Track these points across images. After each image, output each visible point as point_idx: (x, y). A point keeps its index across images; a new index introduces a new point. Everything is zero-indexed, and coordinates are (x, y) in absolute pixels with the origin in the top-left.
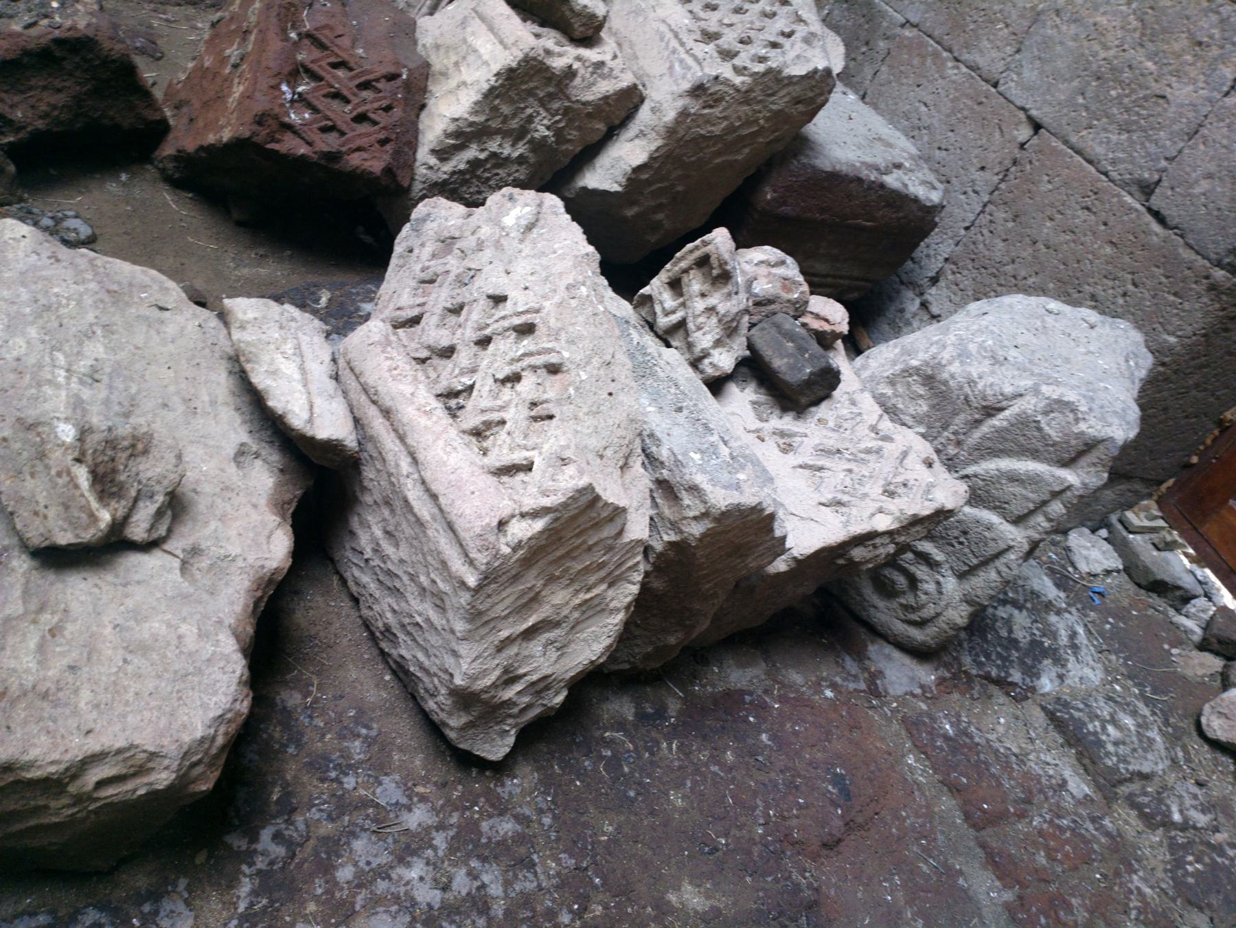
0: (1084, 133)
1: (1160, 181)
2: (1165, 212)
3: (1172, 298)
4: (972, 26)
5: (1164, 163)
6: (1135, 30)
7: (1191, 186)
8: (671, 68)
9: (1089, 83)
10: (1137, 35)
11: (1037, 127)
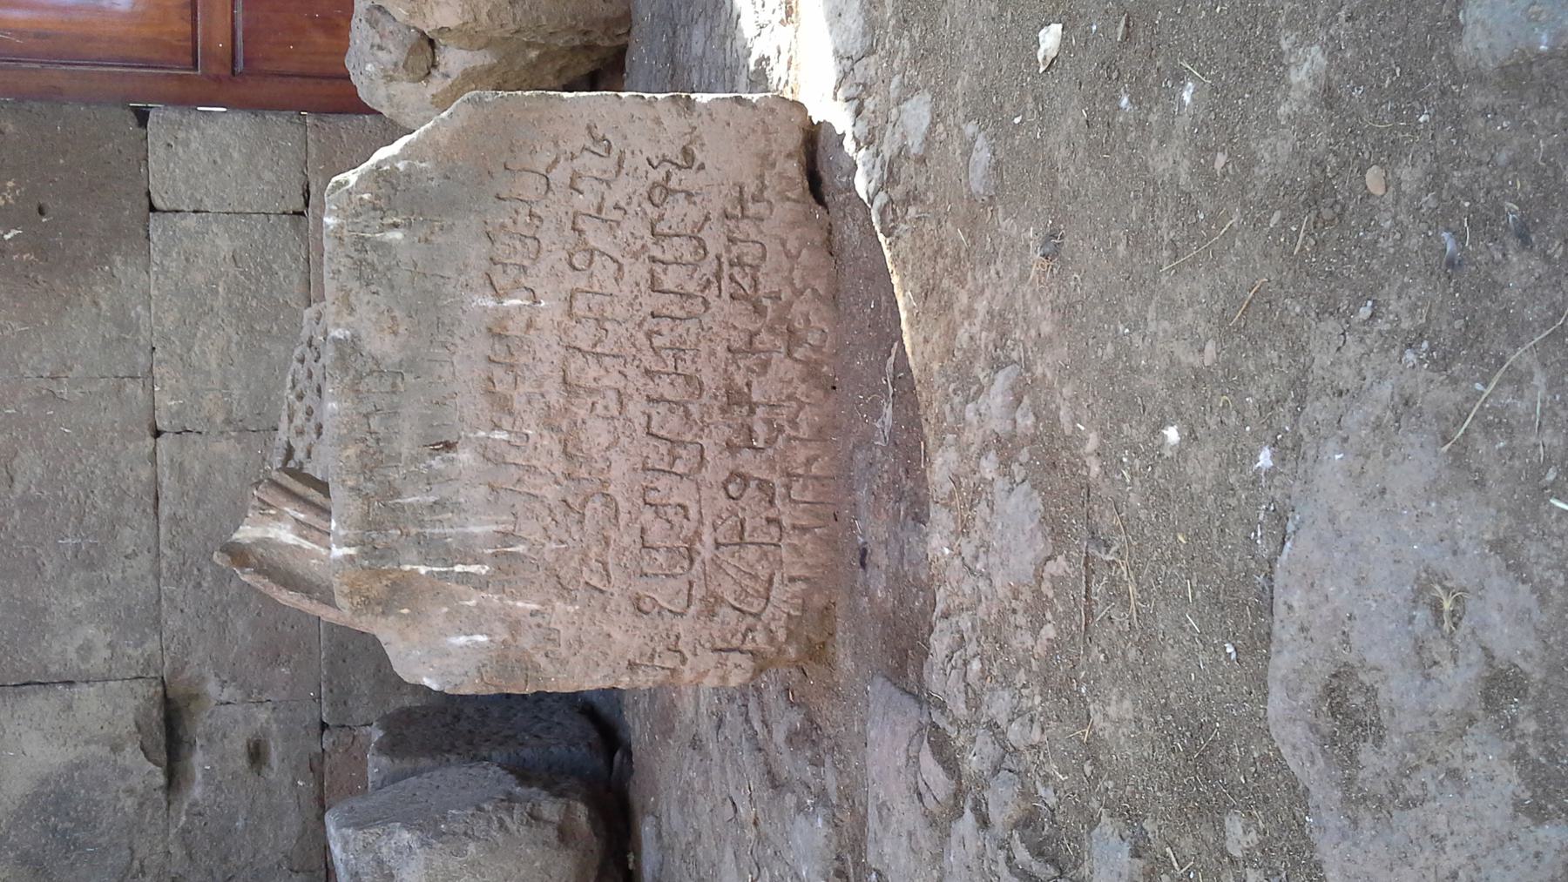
0: (293, 305)
3: (344, 136)
6: (206, 324)
7: (273, 184)
9: (260, 331)
10: (207, 319)
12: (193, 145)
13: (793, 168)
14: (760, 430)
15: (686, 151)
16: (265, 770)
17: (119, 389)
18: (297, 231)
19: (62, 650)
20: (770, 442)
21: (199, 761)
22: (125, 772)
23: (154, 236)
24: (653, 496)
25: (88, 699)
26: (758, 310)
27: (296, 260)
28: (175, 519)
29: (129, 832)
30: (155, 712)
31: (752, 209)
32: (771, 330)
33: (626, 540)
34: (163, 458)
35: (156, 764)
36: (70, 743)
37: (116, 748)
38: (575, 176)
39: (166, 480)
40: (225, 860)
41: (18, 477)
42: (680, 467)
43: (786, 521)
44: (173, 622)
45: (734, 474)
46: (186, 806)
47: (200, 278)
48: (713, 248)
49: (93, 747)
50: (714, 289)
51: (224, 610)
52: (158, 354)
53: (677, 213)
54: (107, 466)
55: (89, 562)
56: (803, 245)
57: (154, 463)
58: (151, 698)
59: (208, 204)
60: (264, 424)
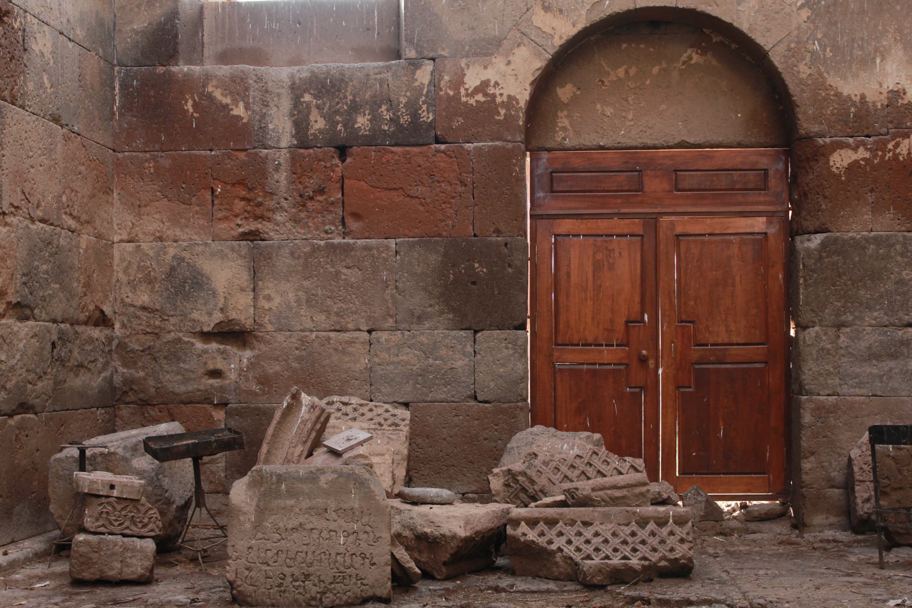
0: (430, 395)
1: (475, 392)
2: (487, 399)
4: (337, 388)
5: (472, 386)
8: (389, 438)
10: (424, 355)
12: (505, 350)
13: (370, 593)
14: (297, 584)
15: (374, 564)
16: (207, 377)
17: (391, 316)
18: (466, 398)
19: (269, 287)
20: (294, 586)
22: (210, 314)
23: (462, 333)
24: (280, 552)
26: (332, 583)
27: (453, 396)
28: (329, 338)
29: (181, 315)
30: (237, 328)
31: (359, 582)
32: (325, 587)
33: (268, 545)
34: (356, 334)
35: (214, 327)
36: (225, 290)
38: (367, 533)
39: (346, 336)
40: (165, 358)
41: (350, 271)
42: (288, 560)
43: (271, 591)
44: (280, 337)
45: (285, 576)
46: (192, 340)
47: (443, 352)
48: (348, 571)
49: (223, 300)
50: (336, 570)
51: (285, 360)
52: (407, 333)
53: (358, 560)
54: (354, 309)
56: (349, 597)
57: (356, 330)
58: (244, 326)
59: (478, 357)
60: (372, 380)
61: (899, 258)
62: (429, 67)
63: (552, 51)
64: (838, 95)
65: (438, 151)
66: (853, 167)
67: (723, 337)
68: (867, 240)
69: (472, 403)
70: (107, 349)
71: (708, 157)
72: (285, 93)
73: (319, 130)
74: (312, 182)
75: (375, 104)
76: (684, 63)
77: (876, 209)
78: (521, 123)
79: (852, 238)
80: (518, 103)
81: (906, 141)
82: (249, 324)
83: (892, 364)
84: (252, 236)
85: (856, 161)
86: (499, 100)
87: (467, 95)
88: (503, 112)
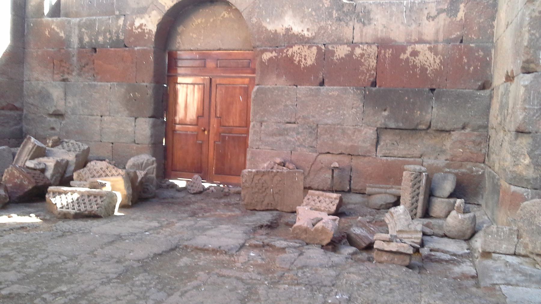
11: (112, 143)
19: (70, 99)
21: (53, 119)
22: (52, 107)
23: (131, 118)
25: (62, 103)
37: (55, 106)
39: (94, 117)
44: (73, 117)
52: (113, 118)
55: (82, 104)
61: (286, 96)
62: (123, 18)
63: (165, 12)
64: (266, 30)
65: (125, 50)
66: (271, 59)
67: (231, 124)
68: (274, 88)
69: (134, 144)
70: (18, 118)
71: (230, 54)
72: (77, 28)
73: (87, 42)
74: (84, 61)
75: (105, 32)
76: (222, 17)
77: (279, 76)
78: (153, 40)
79: (269, 88)
80: (152, 32)
81: (291, 49)
82: (63, 112)
83: (281, 137)
84: (64, 80)
85: (272, 57)
86: (146, 31)
87: (135, 29)
88: (147, 36)
